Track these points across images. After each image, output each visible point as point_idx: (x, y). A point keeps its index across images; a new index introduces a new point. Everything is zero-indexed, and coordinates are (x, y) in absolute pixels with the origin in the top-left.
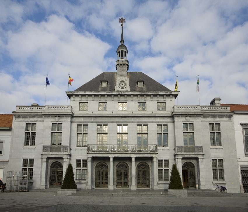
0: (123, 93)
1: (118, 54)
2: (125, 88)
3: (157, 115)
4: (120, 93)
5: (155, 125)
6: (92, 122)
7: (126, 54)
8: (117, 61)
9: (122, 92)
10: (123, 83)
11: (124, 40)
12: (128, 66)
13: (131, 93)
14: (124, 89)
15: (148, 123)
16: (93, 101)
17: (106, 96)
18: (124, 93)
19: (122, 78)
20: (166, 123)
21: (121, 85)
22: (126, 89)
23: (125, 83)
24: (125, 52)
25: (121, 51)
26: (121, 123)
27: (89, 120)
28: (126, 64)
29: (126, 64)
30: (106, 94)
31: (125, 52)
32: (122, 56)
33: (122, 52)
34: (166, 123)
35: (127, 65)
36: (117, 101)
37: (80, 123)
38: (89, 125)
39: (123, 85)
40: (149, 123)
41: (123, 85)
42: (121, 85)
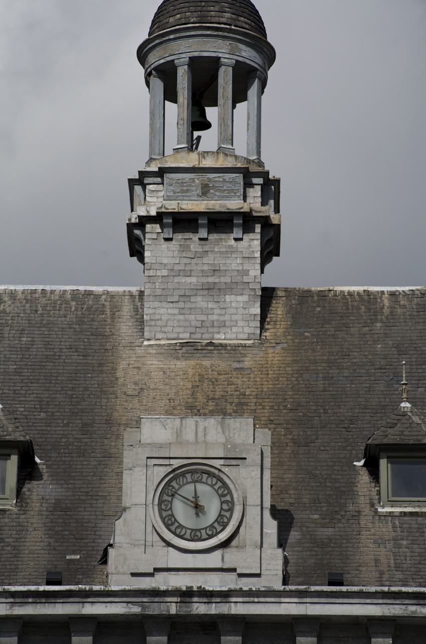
0: (200, 608)
2: (225, 544)
4: (173, 610)
9: (187, 595)
10: (206, 492)
13: (290, 608)
14: (214, 560)
18: (214, 609)
19: (189, 435)
21: (182, 512)
22: (231, 557)
23: (224, 491)
39: (198, 508)
41: (198, 508)
42: (182, 512)
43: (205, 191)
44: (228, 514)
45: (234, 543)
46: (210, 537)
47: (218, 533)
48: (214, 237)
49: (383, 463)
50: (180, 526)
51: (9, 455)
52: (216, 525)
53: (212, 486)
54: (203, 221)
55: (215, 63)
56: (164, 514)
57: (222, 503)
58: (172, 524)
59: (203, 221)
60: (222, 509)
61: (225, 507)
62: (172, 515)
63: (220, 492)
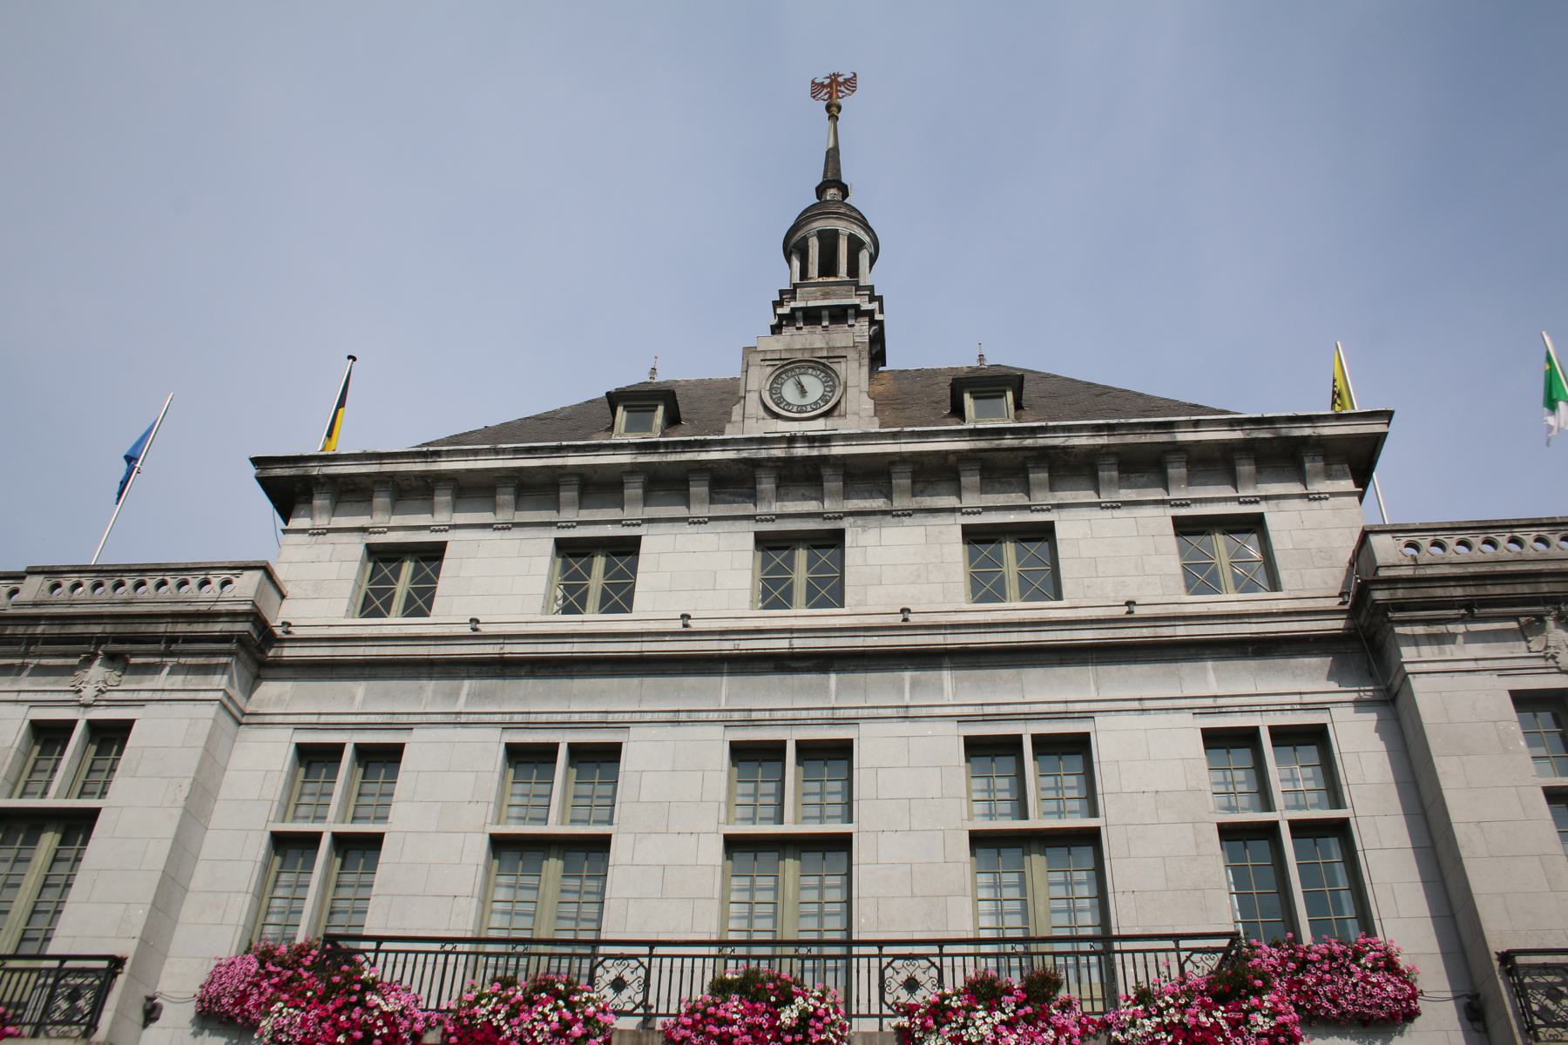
0: (800, 451)
1: (796, 263)
3: (1182, 631)
5: (1186, 735)
6: (457, 721)
7: (864, 257)
8: (782, 292)
11: (844, 180)
12: (872, 322)
15: (1088, 716)
16: (507, 534)
17: (633, 490)
20: (1306, 707)
24: (855, 245)
25: (821, 234)
27: (427, 695)
28: (857, 307)
29: (859, 312)
30: (634, 469)
31: (855, 245)
33: (829, 241)
34: (1306, 707)
35: (870, 313)
36: (745, 523)
37: (327, 727)
38: (419, 750)
40: (1099, 718)
42: (789, 392)
43: (825, 296)
44: (830, 394)
45: (836, 413)
46: (814, 410)
47: (821, 407)
48: (832, 327)
49: (967, 397)
50: (788, 404)
51: (657, 406)
52: (819, 402)
53: (817, 376)
54: (825, 313)
55: (835, 234)
56: (774, 397)
57: (825, 387)
58: (781, 403)
59: (825, 313)
60: (825, 391)
61: (828, 389)
62: (782, 397)
63: (823, 380)
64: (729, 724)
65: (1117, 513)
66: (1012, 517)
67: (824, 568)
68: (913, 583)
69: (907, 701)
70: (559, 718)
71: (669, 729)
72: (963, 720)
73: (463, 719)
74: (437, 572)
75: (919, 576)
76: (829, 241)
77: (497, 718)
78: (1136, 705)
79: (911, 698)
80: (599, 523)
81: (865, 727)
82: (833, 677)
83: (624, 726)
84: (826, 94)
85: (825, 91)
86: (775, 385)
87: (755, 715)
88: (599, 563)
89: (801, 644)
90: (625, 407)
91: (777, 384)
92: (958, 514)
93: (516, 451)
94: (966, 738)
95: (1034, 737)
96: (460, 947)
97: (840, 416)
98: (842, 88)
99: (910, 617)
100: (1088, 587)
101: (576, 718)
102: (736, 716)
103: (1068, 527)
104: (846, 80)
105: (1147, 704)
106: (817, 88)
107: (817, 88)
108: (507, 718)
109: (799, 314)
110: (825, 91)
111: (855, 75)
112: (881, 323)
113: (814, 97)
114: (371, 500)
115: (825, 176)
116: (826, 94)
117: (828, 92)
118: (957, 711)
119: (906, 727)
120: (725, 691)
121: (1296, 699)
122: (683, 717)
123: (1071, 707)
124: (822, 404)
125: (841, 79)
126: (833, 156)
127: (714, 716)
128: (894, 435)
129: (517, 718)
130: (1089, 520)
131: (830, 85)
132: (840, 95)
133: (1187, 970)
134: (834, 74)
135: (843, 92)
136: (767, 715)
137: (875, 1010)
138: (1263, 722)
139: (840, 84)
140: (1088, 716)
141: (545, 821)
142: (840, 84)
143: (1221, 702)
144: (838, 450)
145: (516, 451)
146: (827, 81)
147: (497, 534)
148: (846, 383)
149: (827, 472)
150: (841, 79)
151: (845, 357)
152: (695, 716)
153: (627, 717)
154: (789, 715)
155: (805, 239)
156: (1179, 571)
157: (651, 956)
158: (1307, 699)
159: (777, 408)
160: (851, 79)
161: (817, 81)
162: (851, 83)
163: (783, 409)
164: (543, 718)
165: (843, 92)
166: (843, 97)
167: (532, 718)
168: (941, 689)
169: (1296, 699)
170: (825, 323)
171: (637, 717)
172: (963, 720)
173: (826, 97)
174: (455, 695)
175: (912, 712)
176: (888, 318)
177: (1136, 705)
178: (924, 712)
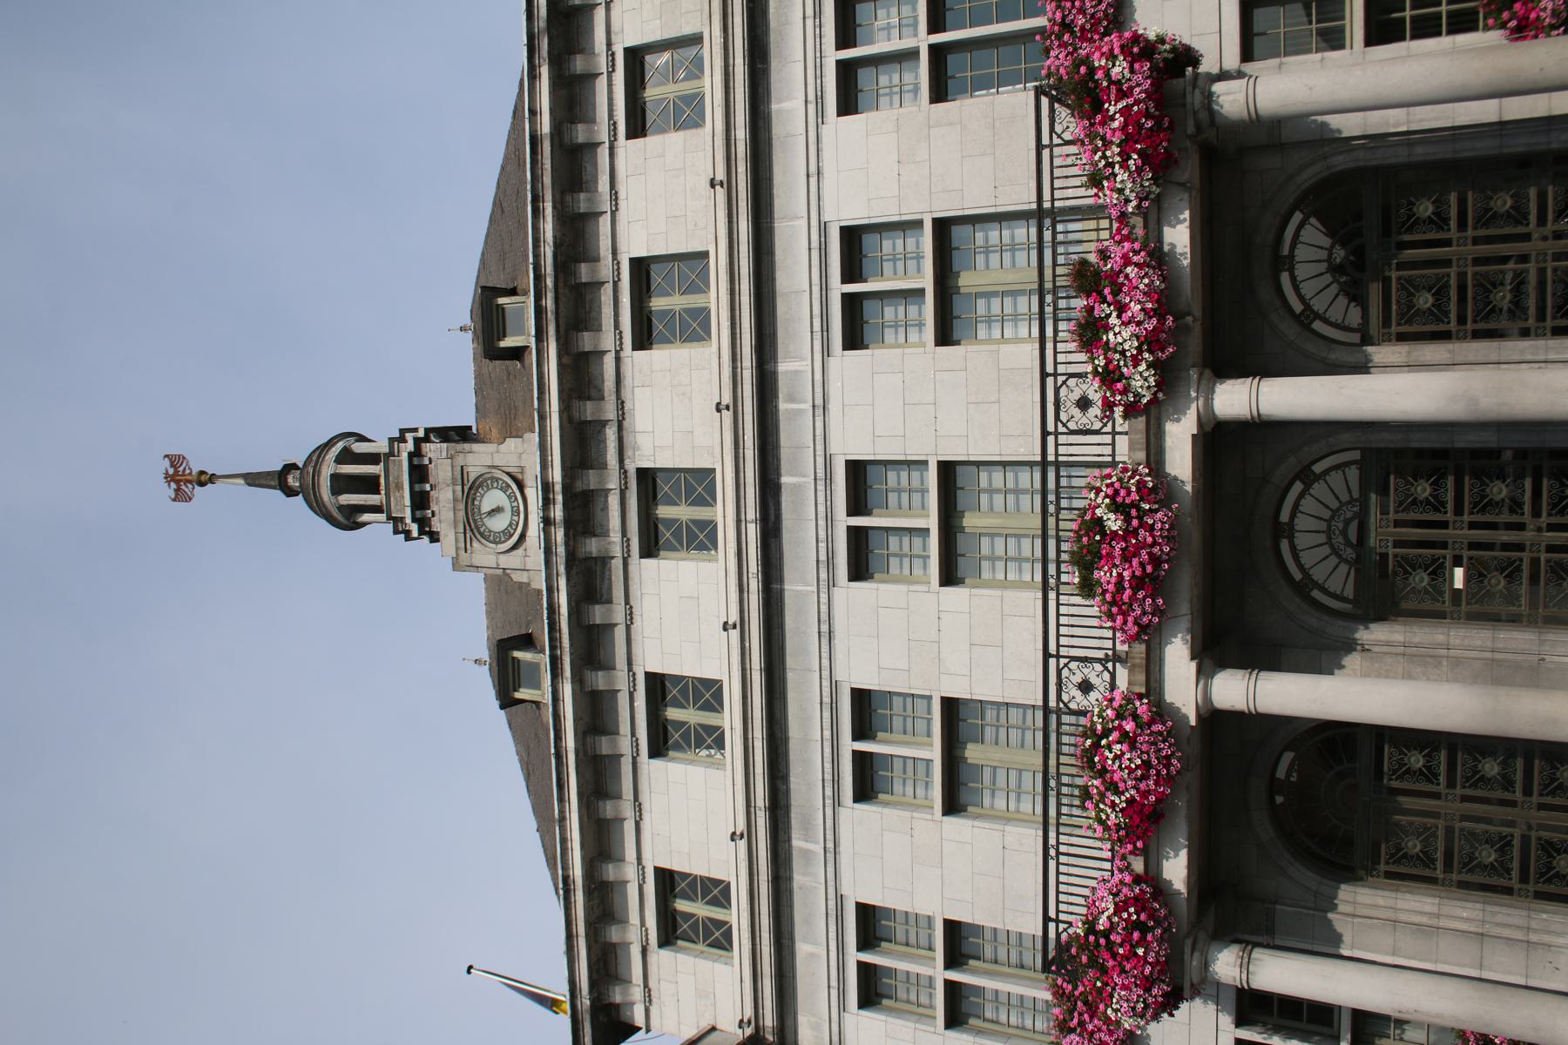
0: (558, 512)
1: (366, 517)
3: (741, 134)
5: (843, 131)
6: (833, 851)
7: (360, 448)
8: (396, 532)
11: (279, 468)
12: (426, 439)
15: (824, 228)
16: (646, 807)
17: (599, 680)
24: (347, 456)
25: (336, 491)
26: (830, 540)
27: (808, 882)
28: (411, 455)
29: (416, 453)
30: (578, 680)
31: (347, 456)
32: (369, 484)
33: (342, 484)
35: (417, 441)
36: (632, 568)
38: (862, 888)
39: (497, 510)
40: (826, 217)
41: (497, 510)
42: (498, 524)
43: (399, 487)
44: (500, 482)
45: (520, 476)
46: (516, 499)
47: (514, 492)
48: (432, 480)
49: (503, 344)
50: (510, 525)
51: (514, 658)
52: (508, 493)
53: (482, 496)
54: (417, 487)
55: (335, 477)
56: (503, 539)
57: (493, 488)
58: (509, 532)
59: (417, 487)
60: (497, 488)
61: (495, 485)
62: (503, 531)
63: (485, 489)
64: (832, 583)
65: (622, 195)
66: (625, 300)
67: (676, 488)
68: (690, 399)
69: (808, 406)
70: (828, 750)
71: (837, 642)
72: (827, 351)
73: (830, 845)
74: (685, 876)
75: (683, 394)
76: (342, 484)
77: (829, 811)
78: (813, 180)
79: (805, 402)
80: (633, 714)
81: (834, 448)
82: (785, 480)
83: (835, 686)
84: (187, 487)
85: (183, 487)
86: (491, 538)
87: (823, 557)
88: (673, 713)
89: (751, 512)
90: (515, 690)
91: (490, 536)
92: (622, 354)
93: (561, 800)
94: (845, 348)
95: (844, 281)
96: (1052, 841)
97: (522, 473)
98: (181, 469)
99: (724, 402)
100: (695, 226)
101: (827, 734)
102: (823, 575)
103: (636, 244)
104: (172, 465)
105: (813, 169)
106: (180, 496)
107: (180, 496)
108: (829, 802)
109: (419, 514)
110: (183, 487)
111: (167, 456)
112: (428, 431)
113: (190, 499)
114: (614, 945)
115: (274, 488)
116: (187, 487)
117: (185, 484)
118: (818, 357)
119: (834, 407)
120: (799, 586)
121: (810, 22)
122: (825, 628)
123: (815, 244)
124: (510, 491)
125: (171, 471)
126: (253, 479)
127: (824, 599)
128: (542, 418)
129: (829, 792)
130: (629, 222)
131: (178, 482)
132: (188, 471)
133: (1071, 138)
134: (166, 478)
135: (185, 469)
136: (822, 545)
137: (1108, 439)
138: (832, 56)
139: (176, 472)
140: (824, 228)
141: (929, 762)
142: (176, 472)
143: (811, 97)
144: (556, 475)
145: (561, 800)
146: (173, 485)
147: (646, 816)
148: (489, 467)
149: (579, 486)
150: (171, 471)
151: (462, 467)
152: (824, 616)
153: (826, 683)
154: (822, 523)
155: (341, 508)
156: (681, 134)
157: (1058, 656)
158: (810, 12)
159: (515, 535)
160: (170, 460)
161: (173, 496)
162: (175, 461)
163: (515, 530)
164: (828, 766)
165: (185, 469)
166: (190, 469)
167: (828, 777)
168: (797, 372)
169: (810, 22)
170: (428, 487)
171: (826, 674)
172: (827, 351)
173: (190, 486)
174: (807, 854)
175: (819, 401)
176: (423, 423)
177: (813, 180)
178: (819, 390)
